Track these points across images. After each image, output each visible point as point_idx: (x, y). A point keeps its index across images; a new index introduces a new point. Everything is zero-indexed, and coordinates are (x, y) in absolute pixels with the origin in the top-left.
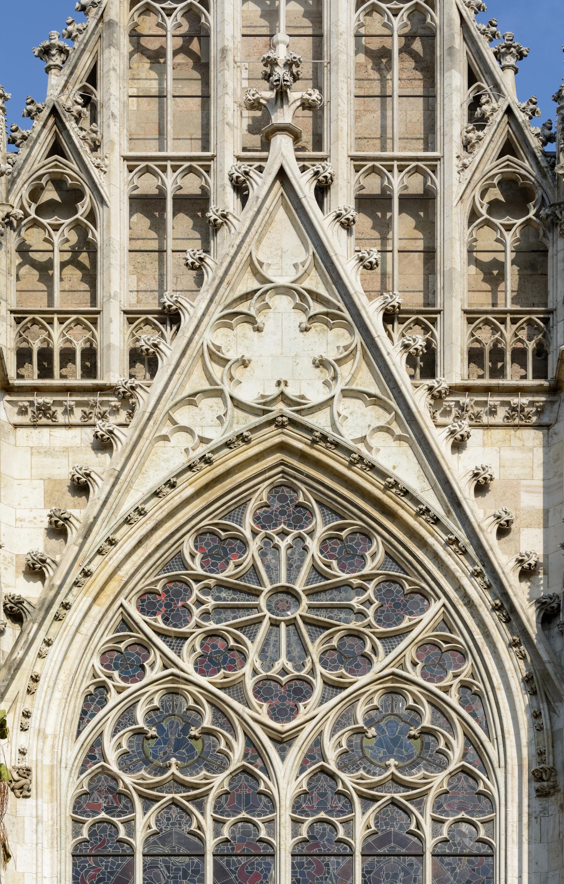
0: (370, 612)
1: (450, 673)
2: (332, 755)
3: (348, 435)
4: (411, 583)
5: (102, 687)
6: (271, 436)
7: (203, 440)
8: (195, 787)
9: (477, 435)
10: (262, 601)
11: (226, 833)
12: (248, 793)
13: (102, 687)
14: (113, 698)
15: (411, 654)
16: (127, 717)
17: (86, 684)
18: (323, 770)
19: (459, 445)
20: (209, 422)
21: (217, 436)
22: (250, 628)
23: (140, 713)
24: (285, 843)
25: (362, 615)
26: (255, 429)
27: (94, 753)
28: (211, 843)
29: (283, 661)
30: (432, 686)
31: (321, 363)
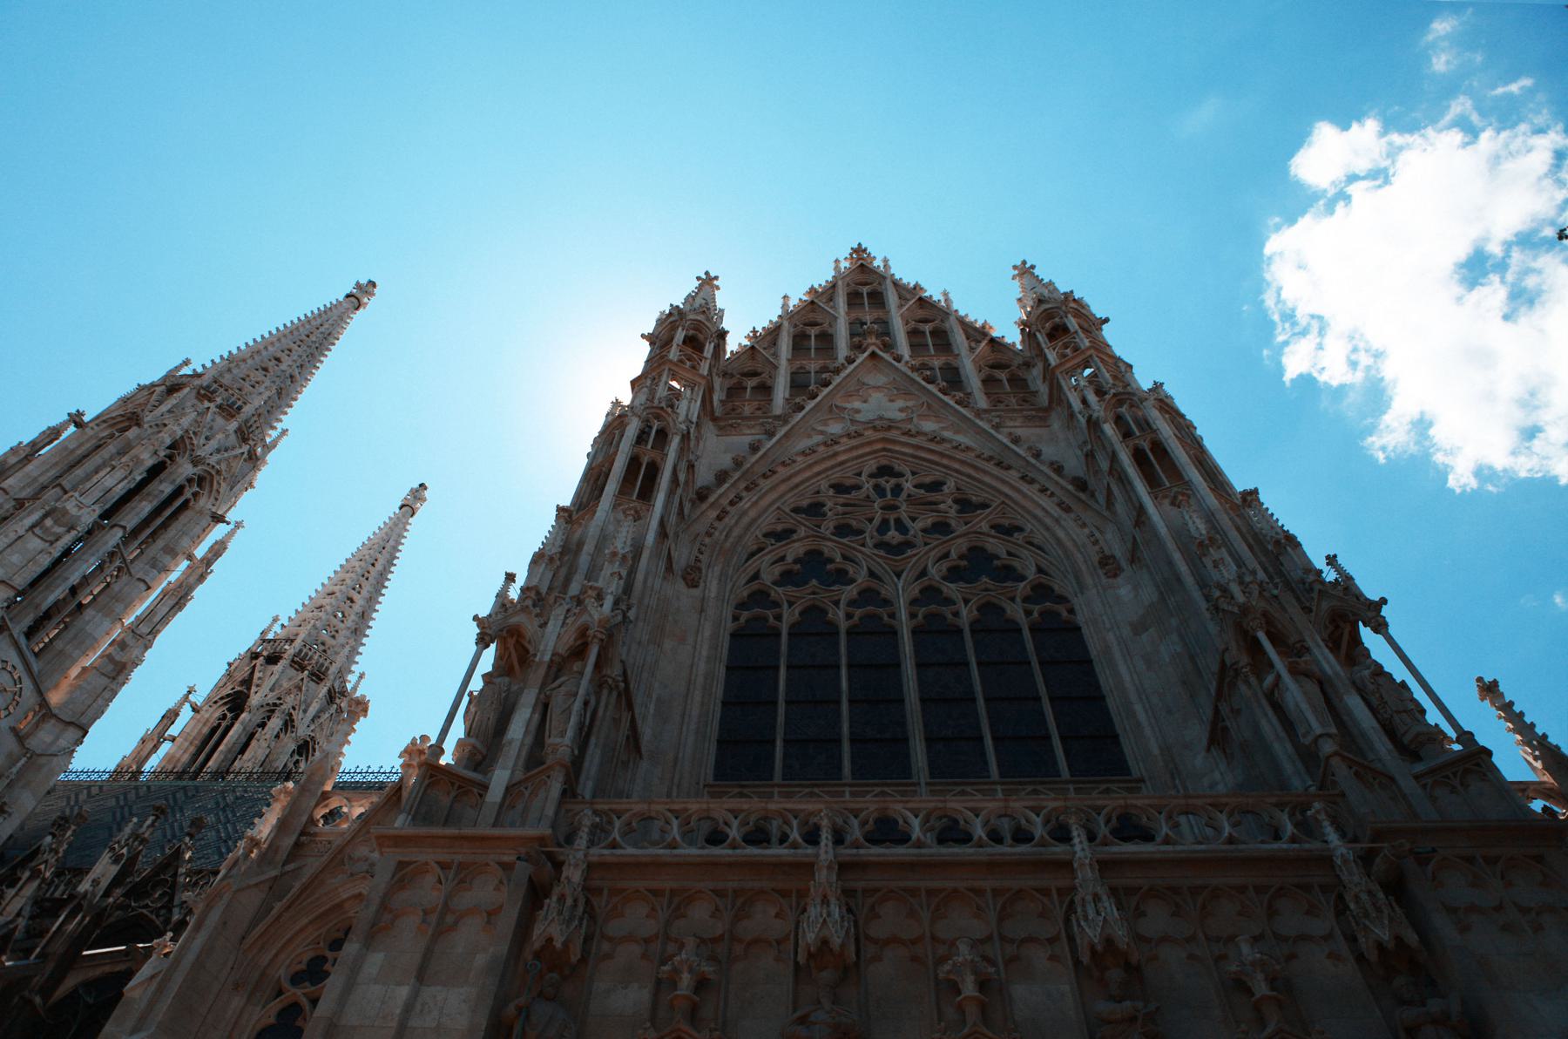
2: (936, 572)
28: (843, 626)
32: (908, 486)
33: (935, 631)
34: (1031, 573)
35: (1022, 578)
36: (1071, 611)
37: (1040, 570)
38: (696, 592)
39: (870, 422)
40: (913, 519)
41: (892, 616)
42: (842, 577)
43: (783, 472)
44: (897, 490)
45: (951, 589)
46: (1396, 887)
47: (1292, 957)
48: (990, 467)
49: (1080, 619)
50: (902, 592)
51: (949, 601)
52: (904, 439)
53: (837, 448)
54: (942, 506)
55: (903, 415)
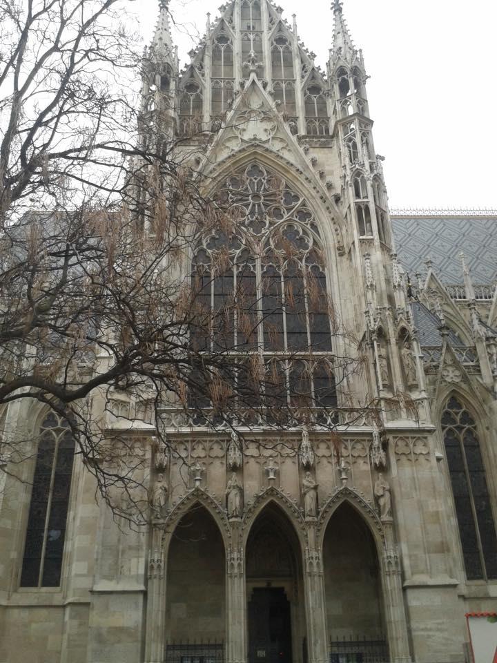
0: (282, 201)
1: (307, 220)
3: (275, 149)
4: (294, 192)
6: (252, 150)
7: (232, 150)
8: (231, 254)
9: (311, 150)
10: (250, 198)
11: (240, 269)
12: (247, 256)
15: (295, 214)
18: (270, 249)
19: (306, 151)
20: (235, 146)
21: (237, 149)
22: (247, 206)
24: (258, 272)
25: (279, 202)
26: (247, 147)
27: (200, 243)
30: (303, 223)
31: (266, 130)
34: (311, 244)
35: (306, 247)
37: (315, 243)
41: (254, 266)
44: (260, 184)
46: (385, 446)
47: (355, 462)
55: (264, 138)
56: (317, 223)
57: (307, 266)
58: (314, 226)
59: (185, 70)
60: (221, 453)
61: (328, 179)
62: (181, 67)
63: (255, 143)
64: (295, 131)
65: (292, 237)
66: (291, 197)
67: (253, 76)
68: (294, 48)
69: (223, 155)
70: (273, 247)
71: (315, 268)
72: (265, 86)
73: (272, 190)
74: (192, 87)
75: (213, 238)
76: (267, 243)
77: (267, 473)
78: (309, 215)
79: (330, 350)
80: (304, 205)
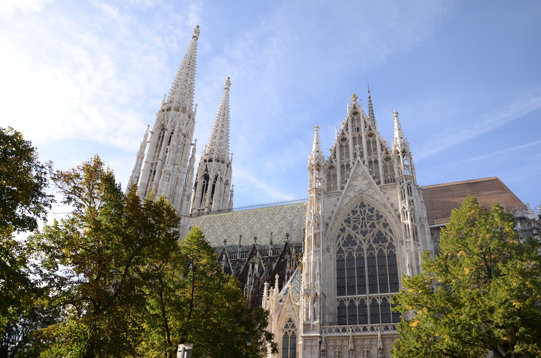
5: (340, 235)
12: (360, 249)
13: (340, 235)
14: (341, 236)
16: (343, 239)
17: (338, 234)
20: (351, 194)
22: (359, 223)
23: (345, 238)
24: (365, 256)
29: (364, 228)
32: (367, 210)
33: (371, 258)
34: (389, 239)
36: (395, 250)
38: (329, 254)
39: (359, 191)
40: (368, 222)
41: (364, 253)
42: (354, 244)
43: (342, 212)
45: (374, 246)
48: (383, 207)
49: (396, 254)
50: (365, 247)
51: (373, 249)
52: (365, 197)
53: (352, 202)
54: (373, 218)
56: (391, 229)
57: (387, 251)
58: (390, 231)
59: (327, 159)
60: (346, 344)
61: (396, 207)
62: (326, 159)
63: (361, 192)
64: (379, 183)
65: (380, 238)
66: (379, 217)
67: (358, 158)
68: (377, 139)
69: (347, 200)
70: (372, 243)
71: (391, 251)
72: (364, 163)
73: (370, 214)
74: (332, 167)
75: (345, 242)
76: (369, 241)
77: (364, 352)
78: (388, 224)
79: (398, 291)
80: (386, 220)
